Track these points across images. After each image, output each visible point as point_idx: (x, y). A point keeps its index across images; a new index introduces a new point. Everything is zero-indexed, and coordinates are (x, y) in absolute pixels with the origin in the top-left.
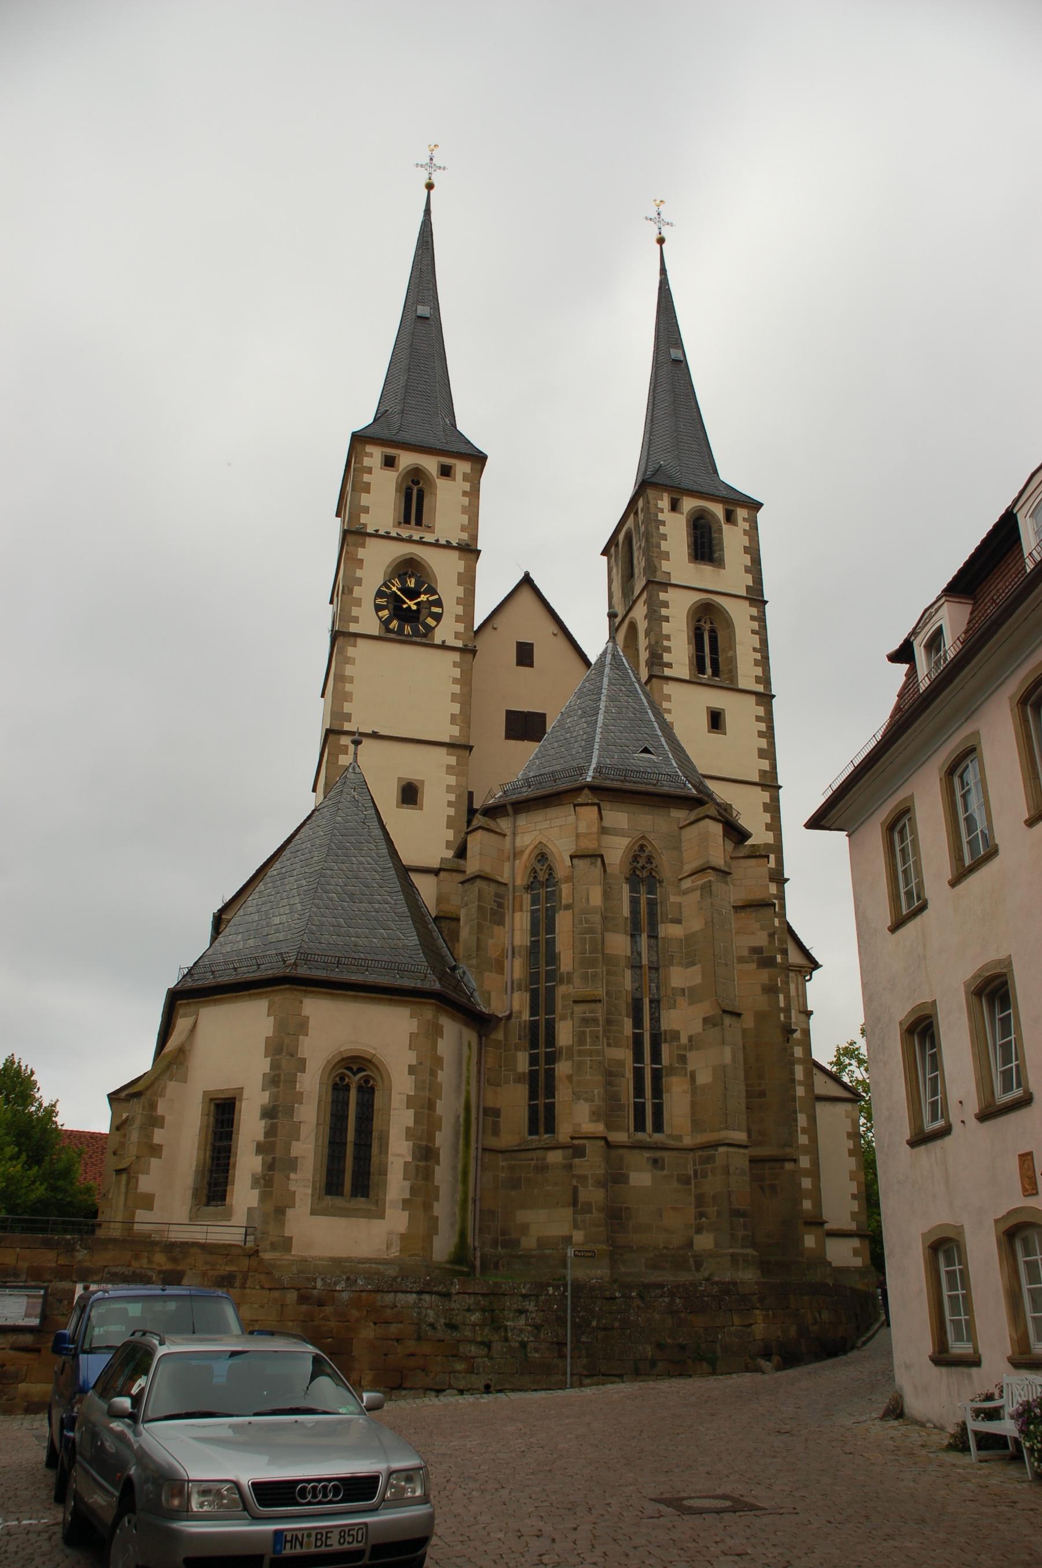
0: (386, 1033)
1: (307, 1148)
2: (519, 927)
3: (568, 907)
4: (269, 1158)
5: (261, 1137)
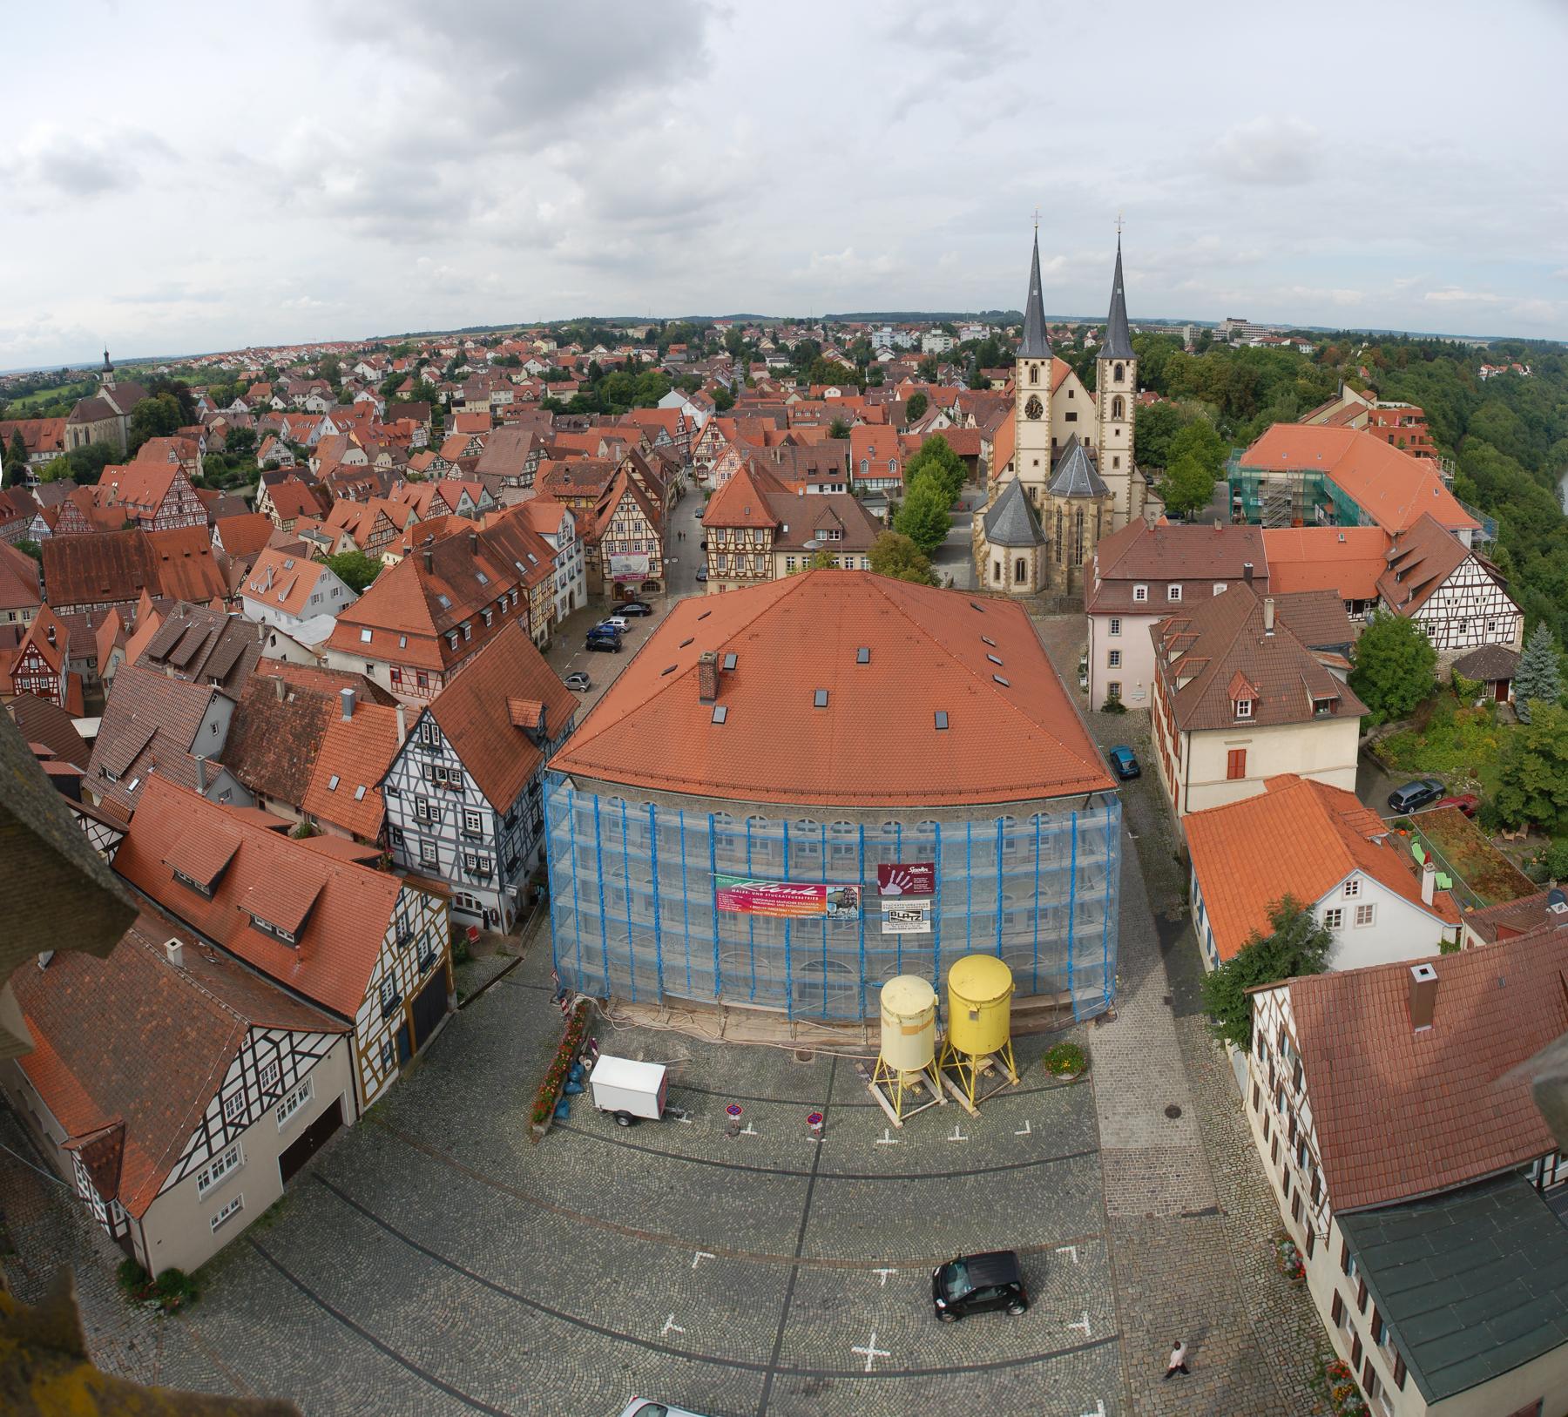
0: (1026, 554)
1: (1013, 575)
2: (1055, 521)
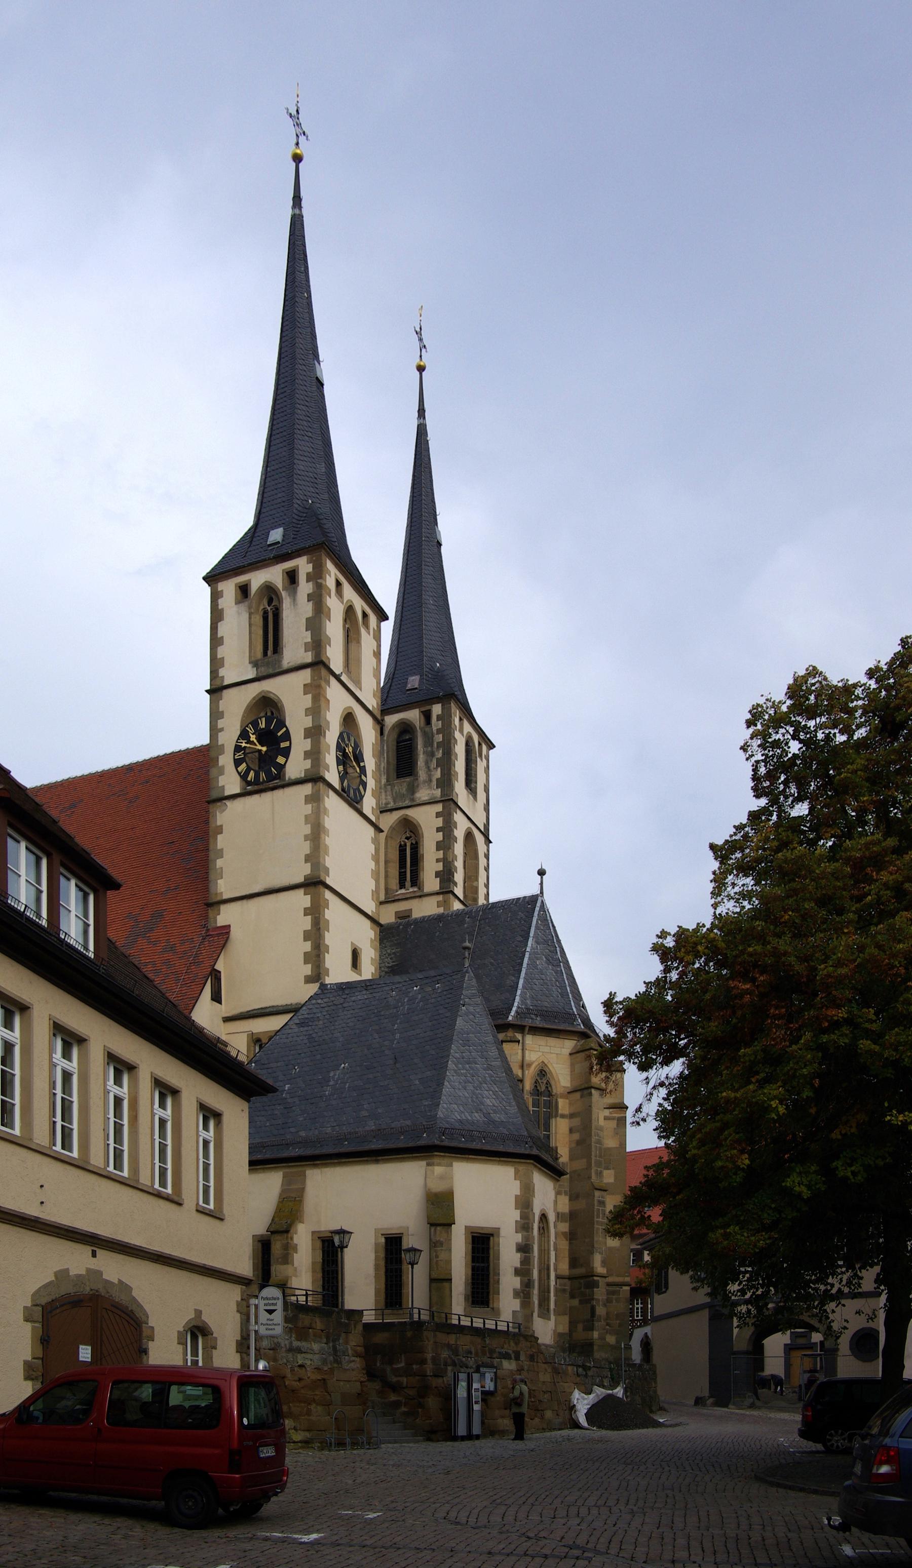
3: (563, 1116)
4: (526, 1279)
5: (519, 1265)
